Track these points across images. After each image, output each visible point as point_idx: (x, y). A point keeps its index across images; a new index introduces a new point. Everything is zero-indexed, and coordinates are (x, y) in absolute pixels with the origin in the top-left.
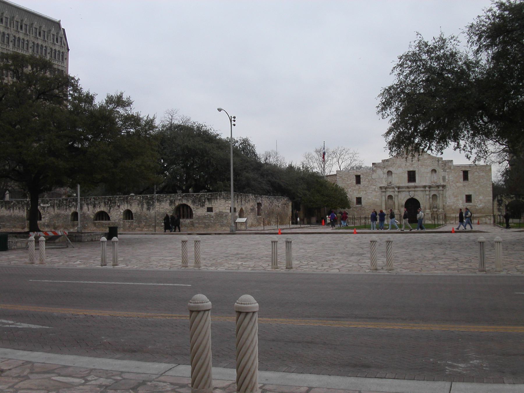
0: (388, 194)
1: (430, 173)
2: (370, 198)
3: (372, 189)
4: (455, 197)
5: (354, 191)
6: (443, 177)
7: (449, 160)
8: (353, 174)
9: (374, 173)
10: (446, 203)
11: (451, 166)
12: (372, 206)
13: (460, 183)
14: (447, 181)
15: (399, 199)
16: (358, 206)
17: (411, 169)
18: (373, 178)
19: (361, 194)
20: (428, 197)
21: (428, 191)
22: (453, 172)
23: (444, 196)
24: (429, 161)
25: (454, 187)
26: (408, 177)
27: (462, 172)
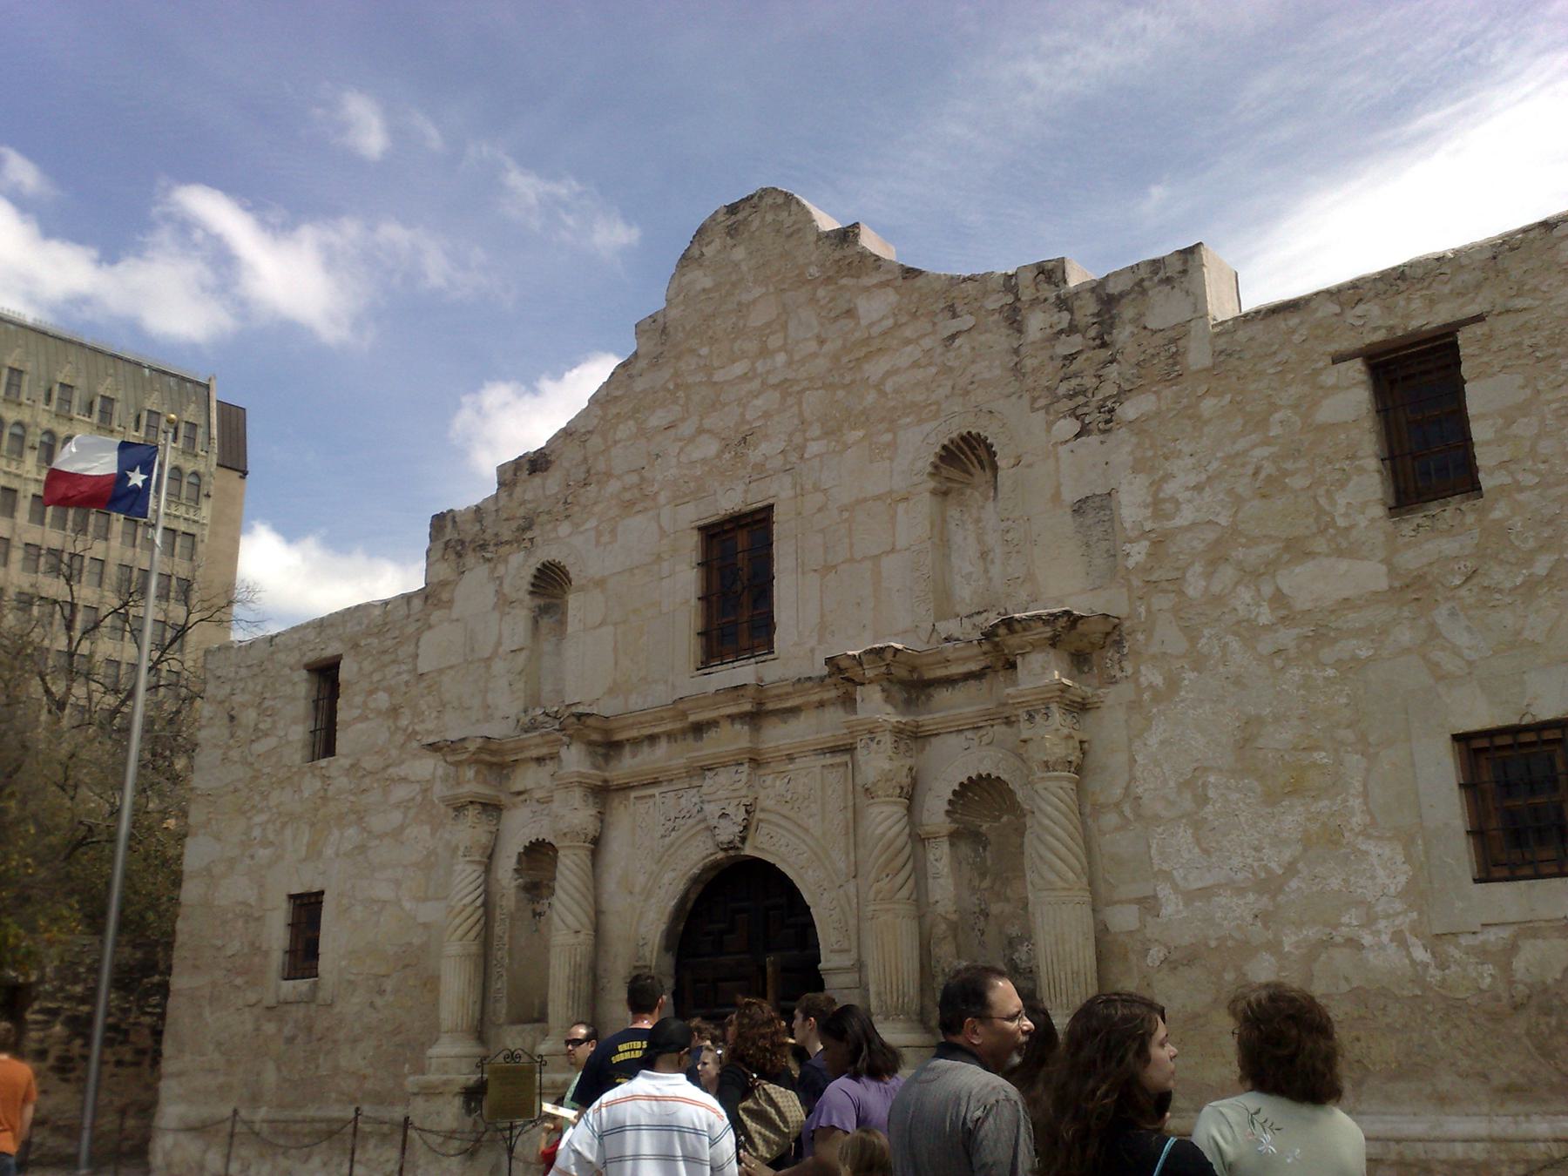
0: (521, 828)
1: (924, 504)
2: (383, 891)
3: (400, 793)
4: (1271, 799)
5: (288, 832)
6: (1079, 508)
7: (1156, 264)
8: (293, 658)
9: (436, 616)
10: (1148, 905)
11: (1177, 337)
12: (389, 985)
13: (1340, 553)
14: (1138, 553)
15: (611, 884)
16: (288, 985)
17: (730, 500)
18: (423, 667)
19: (329, 852)
20: (885, 819)
21: (887, 740)
22: (1208, 406)
23: (1118, 792)
24: (910, 353)
25: (1249, 631)
26: (705, 598)
27: (1356, 370)
